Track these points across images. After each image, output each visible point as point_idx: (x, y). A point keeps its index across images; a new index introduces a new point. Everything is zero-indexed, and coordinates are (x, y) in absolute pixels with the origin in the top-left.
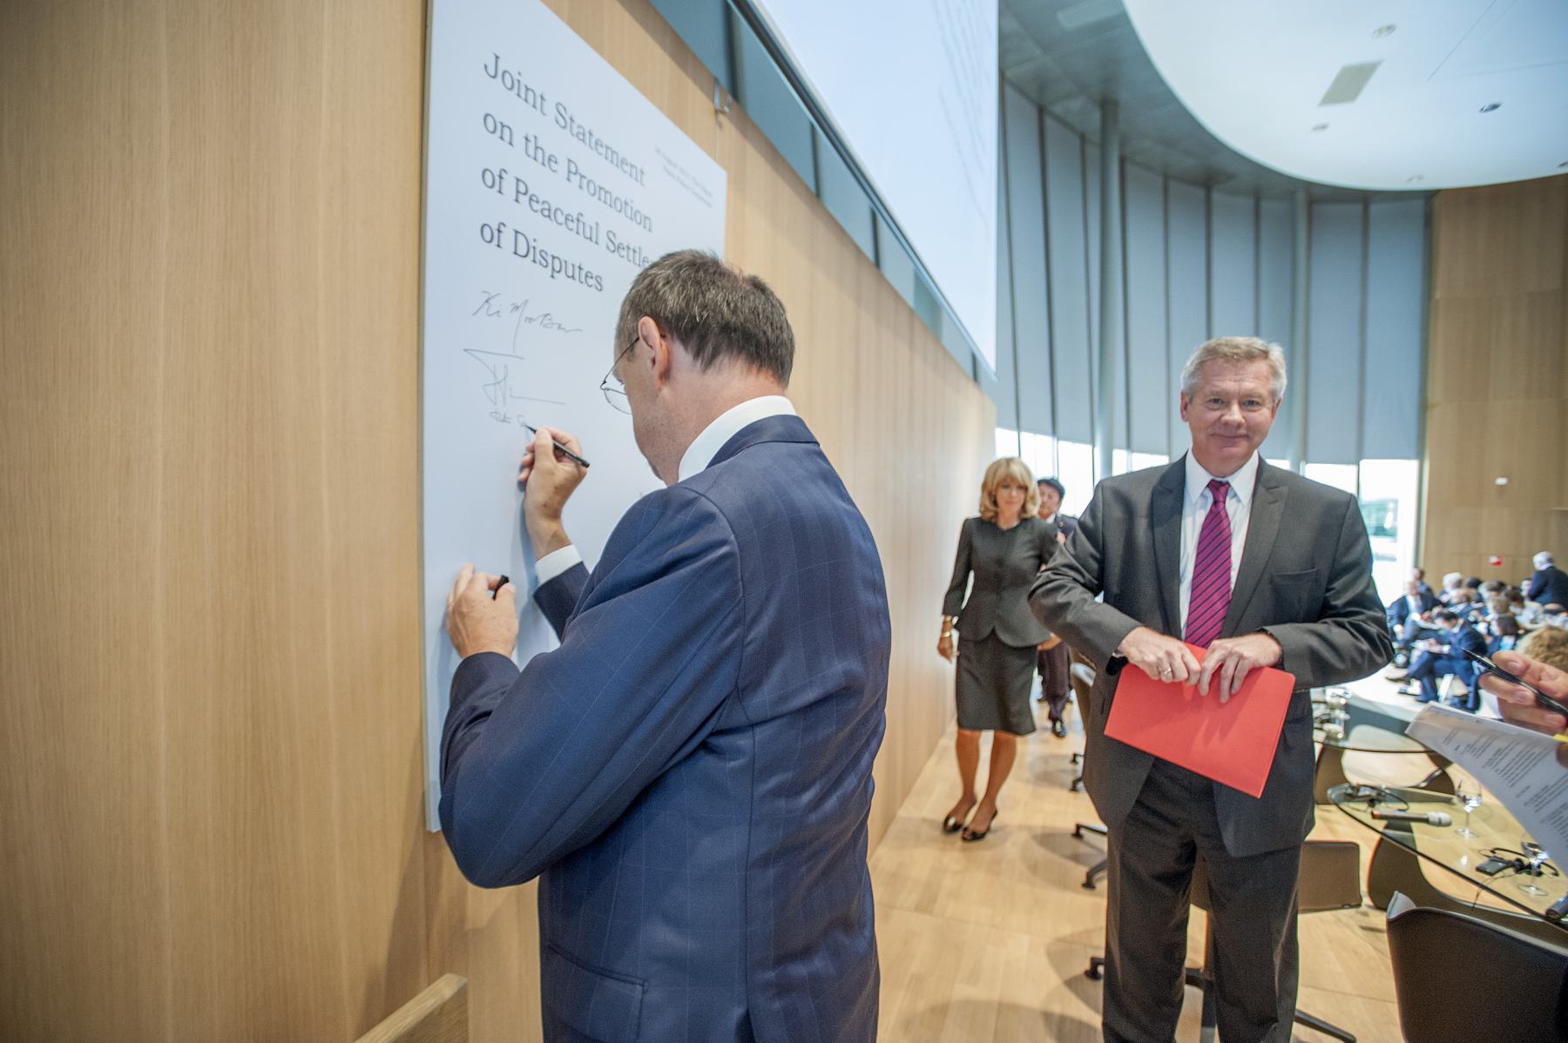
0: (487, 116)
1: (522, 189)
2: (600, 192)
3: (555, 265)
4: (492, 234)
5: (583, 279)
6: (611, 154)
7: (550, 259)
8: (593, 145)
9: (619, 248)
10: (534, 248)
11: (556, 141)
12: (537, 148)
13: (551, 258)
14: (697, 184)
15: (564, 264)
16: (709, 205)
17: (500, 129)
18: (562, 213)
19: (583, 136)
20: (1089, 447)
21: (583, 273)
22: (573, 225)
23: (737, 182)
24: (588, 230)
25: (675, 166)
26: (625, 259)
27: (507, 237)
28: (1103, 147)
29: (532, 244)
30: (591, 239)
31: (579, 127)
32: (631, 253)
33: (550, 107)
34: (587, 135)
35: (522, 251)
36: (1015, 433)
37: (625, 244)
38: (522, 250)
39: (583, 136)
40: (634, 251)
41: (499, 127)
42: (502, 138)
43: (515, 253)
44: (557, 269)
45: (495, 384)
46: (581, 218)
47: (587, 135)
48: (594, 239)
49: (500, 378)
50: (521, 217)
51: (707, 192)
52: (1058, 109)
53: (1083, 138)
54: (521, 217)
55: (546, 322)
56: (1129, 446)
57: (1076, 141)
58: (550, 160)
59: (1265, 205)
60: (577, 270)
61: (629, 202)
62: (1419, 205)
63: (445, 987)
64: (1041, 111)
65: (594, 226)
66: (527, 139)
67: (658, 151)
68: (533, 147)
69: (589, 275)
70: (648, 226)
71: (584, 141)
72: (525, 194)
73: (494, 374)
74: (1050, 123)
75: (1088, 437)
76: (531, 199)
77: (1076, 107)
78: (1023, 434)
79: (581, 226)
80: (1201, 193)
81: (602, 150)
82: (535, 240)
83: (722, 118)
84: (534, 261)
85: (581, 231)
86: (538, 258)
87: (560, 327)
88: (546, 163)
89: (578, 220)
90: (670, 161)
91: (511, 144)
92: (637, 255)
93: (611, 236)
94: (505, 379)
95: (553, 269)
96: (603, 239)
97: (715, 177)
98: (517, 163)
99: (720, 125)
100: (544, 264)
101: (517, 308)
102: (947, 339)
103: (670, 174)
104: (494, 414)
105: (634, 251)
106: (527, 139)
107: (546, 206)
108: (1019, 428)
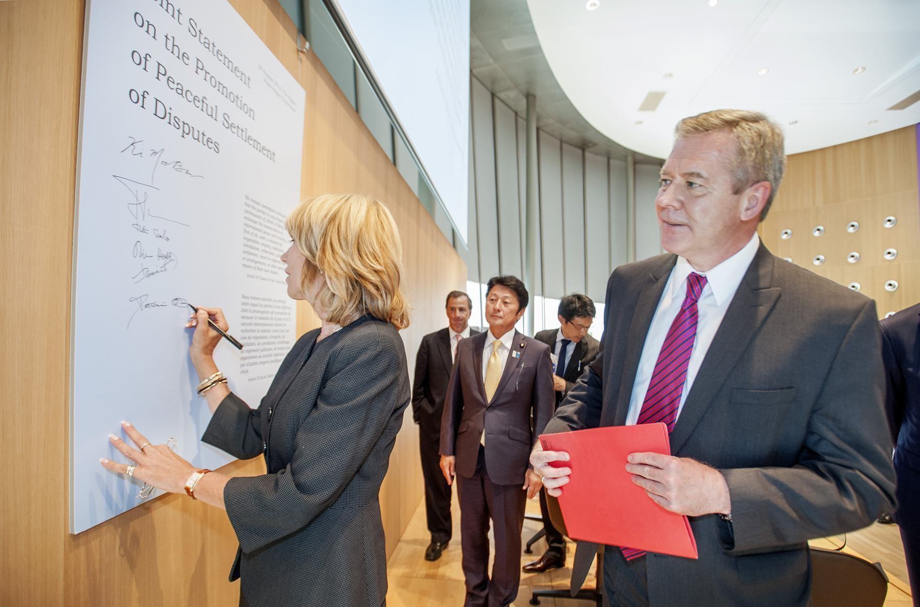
0: (136, 13)
1: (162, 71)
2: (219, 85)
3: (185, 129)
4: (139, 98)
5: (205, 143)
6: (227, 61)
7: (181, 124)
8: (215, 54)
9: (231, 126)
10: (170, 114)
11: (187, 43)
12: (174, 45)
13: (182, 123)
14: (286, 95)
15: (191, 129)
16: (294, 110)
17: (147, 25)
18: (192, 95)
19: (208, 45)
21: (205, 138)
22: (199, 104)
23: (311, 99)
24: (210, 110)
25: (272, 80)
26: (236, 134)
27: (150, 102)
28: (528, 120)
29: (168, 111)
30: (212, 116)
31: (205, 38)
32: (240, 131)
33: (184, 19)
34: (211, 46)
35: (161, 113)
36: (478, 285)
37: (236, 125)
38: (161, 113)
39: (208, 45)
40: (242, 131)
41: (146, 24)
42: (148, 32)
43: (155, 115)
44: (187, 132)
46: (205, 100)
47: (211, 46)
48: (214, 116)
49: (141, 200)
50: (159, 89)
51: (292, 101)
52: (502, 95)
53: (516, 113)
54: (159, 89)
55: (176, 167)
56: (543, 294)
57: (513, 114)
58: (183, 55)
59: (612, 161)
60: (201, 136)
61: (239, 97)
64: (493, 95)
65: (214, 108)
66: (166, 36)
67: (260, 68)
68: (171, 44)
69: (209, 140)
70: (252, 116)
71: (208, 48)
72: (164, 75)
73: (137, 198)
74: (497, 102)
76: (168, 80)
77: (513, 96)
79: (205, 105)
80: (580, 152)
81: (222, 58)
82: (171, 109)
83: (301, 55)
84: (169, 123)
85: (205, 109)
86: (173, 121)
88: (181, 57)
89: (203, 101)
90: (268, 76)
91: (154, 37)
92: (244, 133)
93: (226, 116)
94: (144, 202)
95: (184, 131)
96: (220, 118)
97: (299, 94)
98: (159, 52)
99: (301, 60)
100: (178, 127)
102: (438, 220)
103: (268, 84)
104: (135, 226)
105: (242, 131)
106: (166, 36)
107: (179, 87)
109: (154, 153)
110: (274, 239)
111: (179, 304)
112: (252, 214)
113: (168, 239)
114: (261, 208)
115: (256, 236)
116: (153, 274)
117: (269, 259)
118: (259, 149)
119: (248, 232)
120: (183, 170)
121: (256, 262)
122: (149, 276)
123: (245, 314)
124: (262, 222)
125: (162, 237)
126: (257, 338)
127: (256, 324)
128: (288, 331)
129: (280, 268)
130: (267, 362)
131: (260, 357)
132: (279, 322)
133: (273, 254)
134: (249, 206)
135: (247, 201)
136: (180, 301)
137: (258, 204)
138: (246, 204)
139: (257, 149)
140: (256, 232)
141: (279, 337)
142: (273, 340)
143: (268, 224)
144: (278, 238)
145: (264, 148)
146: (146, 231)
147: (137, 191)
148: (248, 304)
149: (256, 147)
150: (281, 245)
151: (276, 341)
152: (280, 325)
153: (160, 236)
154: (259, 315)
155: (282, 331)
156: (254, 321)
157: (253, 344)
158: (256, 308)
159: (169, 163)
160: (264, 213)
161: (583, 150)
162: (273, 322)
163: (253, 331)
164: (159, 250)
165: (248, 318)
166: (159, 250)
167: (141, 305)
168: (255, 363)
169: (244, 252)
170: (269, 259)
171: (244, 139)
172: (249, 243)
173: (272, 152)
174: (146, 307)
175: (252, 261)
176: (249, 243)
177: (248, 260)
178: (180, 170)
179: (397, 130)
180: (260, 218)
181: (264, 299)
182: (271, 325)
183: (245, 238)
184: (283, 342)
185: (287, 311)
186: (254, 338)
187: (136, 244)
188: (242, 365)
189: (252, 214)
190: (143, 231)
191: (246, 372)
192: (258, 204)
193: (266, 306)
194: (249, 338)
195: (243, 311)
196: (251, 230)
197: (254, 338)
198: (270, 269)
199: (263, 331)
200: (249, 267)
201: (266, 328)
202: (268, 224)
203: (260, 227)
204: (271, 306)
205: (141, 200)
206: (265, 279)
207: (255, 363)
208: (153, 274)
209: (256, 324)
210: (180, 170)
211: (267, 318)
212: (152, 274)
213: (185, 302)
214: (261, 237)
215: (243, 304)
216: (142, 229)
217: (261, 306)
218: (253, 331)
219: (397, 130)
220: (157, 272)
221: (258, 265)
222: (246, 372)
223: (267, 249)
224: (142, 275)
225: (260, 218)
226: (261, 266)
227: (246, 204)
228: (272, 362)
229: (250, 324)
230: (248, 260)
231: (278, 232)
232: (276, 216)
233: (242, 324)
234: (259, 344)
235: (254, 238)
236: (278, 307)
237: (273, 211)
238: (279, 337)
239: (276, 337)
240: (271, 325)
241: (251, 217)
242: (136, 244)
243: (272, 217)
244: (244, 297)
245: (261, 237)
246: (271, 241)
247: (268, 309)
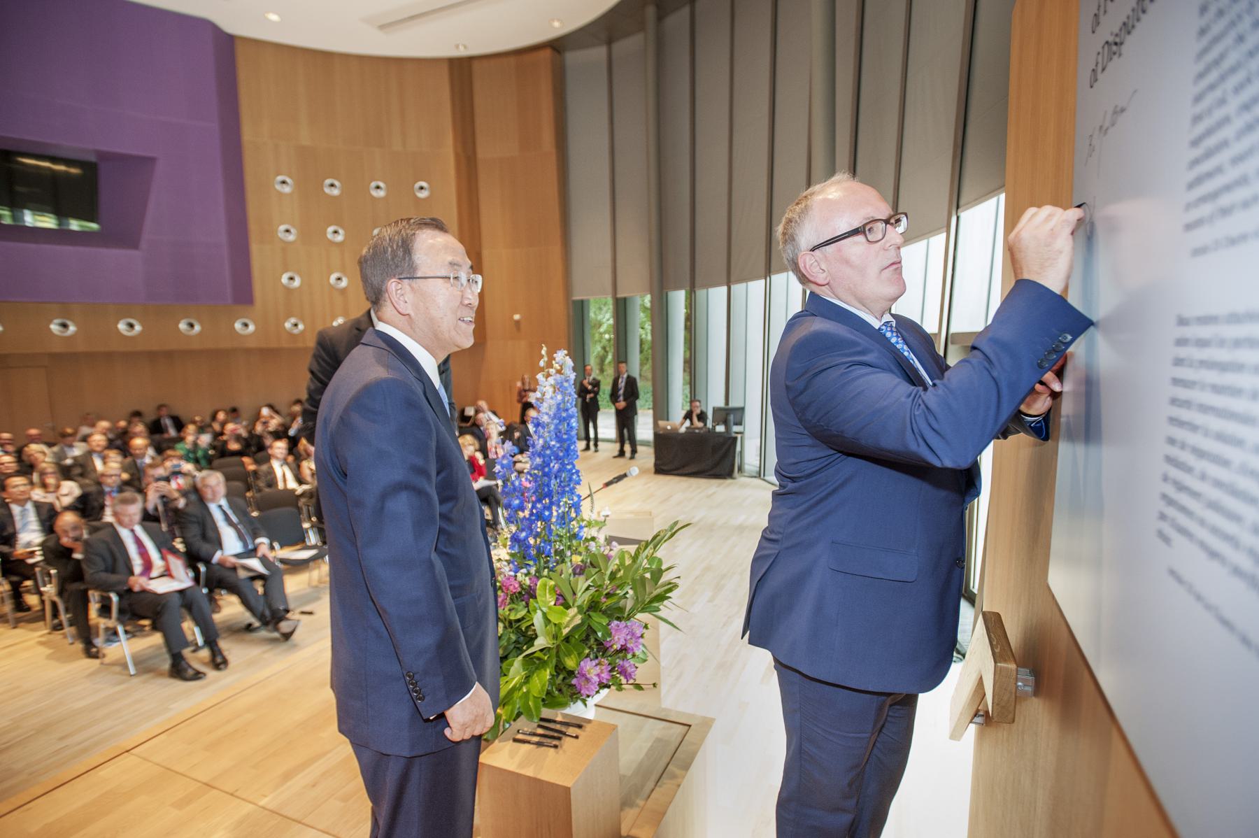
126: (1200, 453)
131: (1202, 522)
181: (1234, 318)
191: (1166, 540)
193: (1237, 343)
199: (1221, 437)
201: (1231, 428)
206: (1243, 238)
217: (1222, 343)
218: (1194, 428)
222: (1166, 540)
226: (1225, 200)
234: (1203, 477)
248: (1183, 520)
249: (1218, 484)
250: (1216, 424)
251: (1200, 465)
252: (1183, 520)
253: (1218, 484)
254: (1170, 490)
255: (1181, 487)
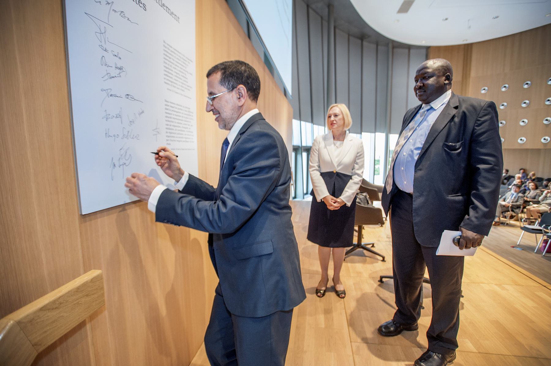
5: (138, 3)
20: (323, 128)
45: (100, 33)
52: (313, 6)
53: (322, 18)
55: (122, 15)
57: (320, 19)
59: (379, 47)
62: (424, 51)
63: (94, 273)
64: (308, 6)
74: (311, 11)
75: (323, 124)
78: (302, 122)
80: (360, 41)
87: (128, 19)
101: (108, 3)
104: (100, 46)
108: (300, 120)
109: (108, 3)
110: (181, 70)
111: (129, 98)
112: (168, 52)
113: (120, 58)
114: (173, 50)
115: (171, 66)
116: (113, 77)
117: (179, 82)
118: (169, 13)
119: (166, 63)
120: (126, 18)
121: (172, 82)
122: (111, 78)
123: (167, 111)
124: (174, 59)
125: (117, 55)
126: (175, 126)
127: (174, 118)
128: (192, 126)
129: (186, 88)
130: (181, 141)
131: (177, 137)
132: (187, 120)
133: (181, 79)
134: (166, 47)
135: (164, 44)
136: (130, 97)
137: (171, 47)
138: (164, 46)
139: (168, 13)
140: (170, 64)
141: (187, 128)
142: (183, 129)
143: (177, 60)
144: (184, 70)
145: (172, 13)
146: (108, 51)
147: (100, 25)
148: (168, 106)
149: (168, 11)
150: (186, 75)
151: (186, 130)
152: (188, 121)
153: (116, 56)
154: (175, 113)
155: (189, 125)
156: (172, 116)
157: (173, 129)
158: (173, 109)
159: (117, 11)
160: (175, 53)
161: (362, 40)
162: (184, 119)
163: (173, 122)
164: (116, 64)
165: (169, 114)
166: (116, 64)
167: (108, 95)
168: (175, 141)
169: (165, 75)
170: (179, 82)
171: (161, 5)
172: (167, 70)
173: (177, 16)
174: (111, 96)
175: (170, 81)
176: (167, 70)
177: (168, 80)
178: (124, 17)
179: (251, 22)
180: (173, 56)
181: (178, 105)
182: (182, 120)
183: (165, 67)
184: (189, 132)
185: (191, 114)
186: (173, 126)
187: (102, 58)
188: (167, 140)
189: (168, 52)
190: (106, 50)
191: (170, 144)
192: (171, 47)
193: (179, 109)
194: (170, 125)
195: (166, 109)
196: (168, 63)
197: (173, 126)
198: (180, 87)
199: (178, 123)
200: (168, 84)
201: (180, 121)
202: (177, 60)
203: (173, 61)
204: (181, 110)
205: (103, 31)
207: (175, 141)
208: (113, 77)
209: (174, 118)
210: (124, 17)
211: (180, 116)
212: (113, 77)
213: (132, 97)
214: (174, 68)
215: (166, 105)
216: (104, 49)
217: (176, 108)
218: (173, 122)
219: (251, 22)
220: (115, 77)
221: (173, 84)
222: (170, 144)
223: (178, 75)
224: (106, 77)
225: (173, 56)
226: (175, 85)
227: (164, 46)
228: (184, 141)
229: (171, 118)
230: (168, 80)
231: (184, 66)
232: (182, 56)
233: (166, 117)
234: (176, 130)
235: (170, 67)
236: (186, 111)
237: (180, 53)
238: (187, 128)
239: (185, 128)
240: (182, 120)
241: (168, 55)
242: (102, 58)
243: (179, 56)
244: (166, 101)
245: (174, 68)
246: (180, 71)
247: (180, 111)
248: (172, 139)
249: (179, 130)
250: (177, 121)
251: (174, 128)
252: (172, 139)
253: (179, 130)
254: (169, 135)
255: (171, 133)
